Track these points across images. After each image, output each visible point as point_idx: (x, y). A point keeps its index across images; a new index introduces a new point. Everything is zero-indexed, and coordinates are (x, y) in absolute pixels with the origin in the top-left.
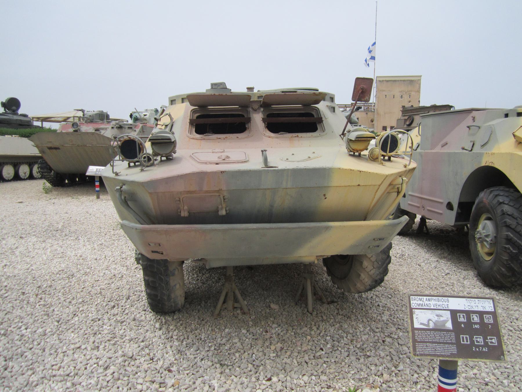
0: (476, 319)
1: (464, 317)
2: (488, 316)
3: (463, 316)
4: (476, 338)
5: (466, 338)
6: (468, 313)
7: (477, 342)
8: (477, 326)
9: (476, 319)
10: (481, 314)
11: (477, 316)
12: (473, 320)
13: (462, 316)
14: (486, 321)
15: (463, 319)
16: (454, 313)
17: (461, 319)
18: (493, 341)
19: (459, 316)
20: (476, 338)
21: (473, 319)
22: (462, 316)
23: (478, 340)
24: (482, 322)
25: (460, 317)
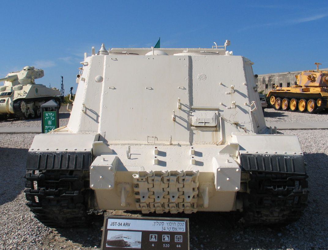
0: (167, 239)
1: (155, 238)
2: (179, 236)
3: (155, 236)
6: (160, 234)
8: (168, 246)
9: (167, 239)
10: (172, 235)
11: (168, 237)
13: (153, 237)
14: (176, 240)
15: (154, 239)
16: (146, 235)
17: (152, 239)
19: (152, 236)
21: (164, 239)
22: (153, 237)
24: (172, 243)
25: (151, 238)
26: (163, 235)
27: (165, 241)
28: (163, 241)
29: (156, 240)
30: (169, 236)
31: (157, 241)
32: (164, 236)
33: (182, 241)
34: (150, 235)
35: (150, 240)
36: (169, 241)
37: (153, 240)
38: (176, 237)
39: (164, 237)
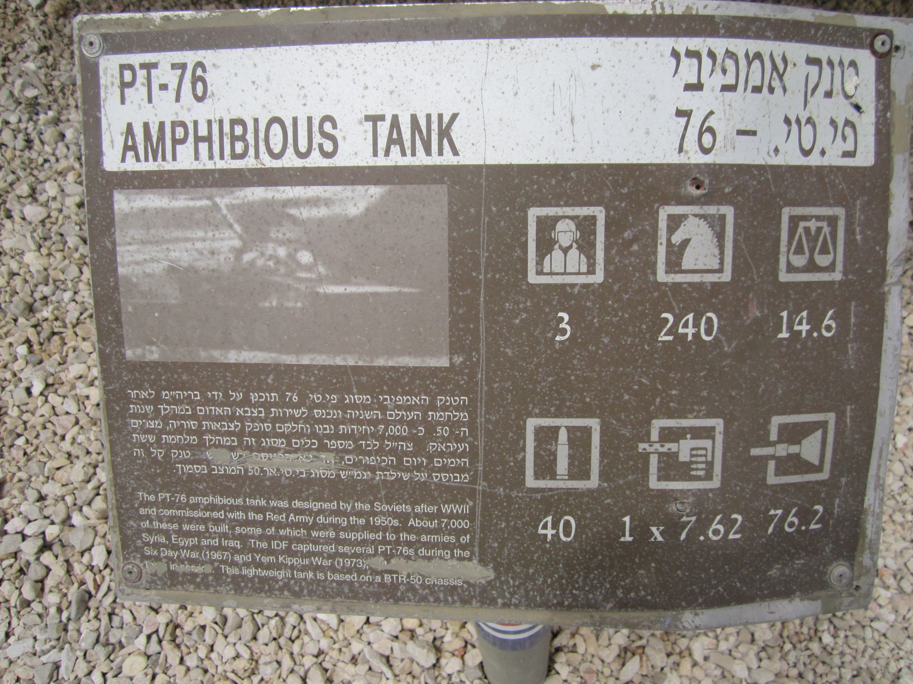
1: (586, 245)
3: (586, 226)
4: (668, 435)
5: (579, 439)
7: (672, 467)
9: (700, 247)
11: (717, 225)
12: (674, 265)
13: (565, 232)
14: (790, 268)
18: (809, 449)
19: (546, 226)
20: (668, 435)
21: (676, 254)
22: (565, 232)
23: (684, 449)
25: (546, 245)
26: (664, 212)
27: (679, 278)
28: (662, 276)
29: (591, 271)
30: (728, 211)
31: (598, 277)
32: (675, 222)
33: (839, 266)
34: (534, 213)
35: (533, 278)
36: (726, 276)
37: (565, 267)
38: (794, 221)
39: (671, 230)
